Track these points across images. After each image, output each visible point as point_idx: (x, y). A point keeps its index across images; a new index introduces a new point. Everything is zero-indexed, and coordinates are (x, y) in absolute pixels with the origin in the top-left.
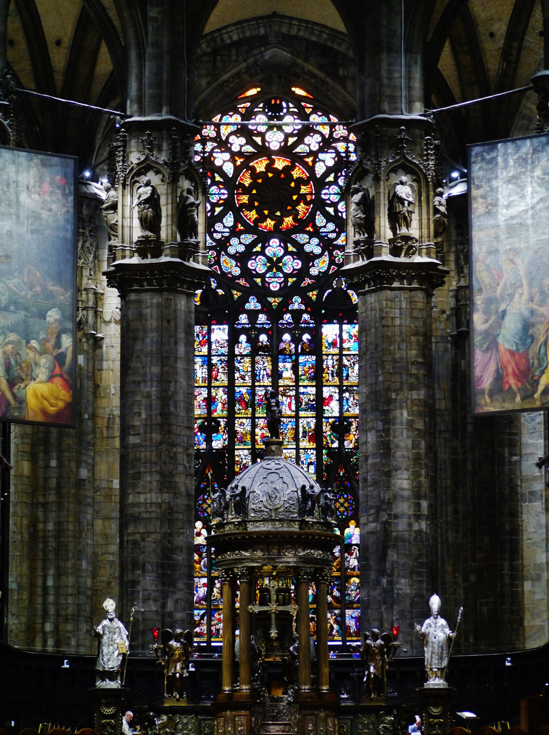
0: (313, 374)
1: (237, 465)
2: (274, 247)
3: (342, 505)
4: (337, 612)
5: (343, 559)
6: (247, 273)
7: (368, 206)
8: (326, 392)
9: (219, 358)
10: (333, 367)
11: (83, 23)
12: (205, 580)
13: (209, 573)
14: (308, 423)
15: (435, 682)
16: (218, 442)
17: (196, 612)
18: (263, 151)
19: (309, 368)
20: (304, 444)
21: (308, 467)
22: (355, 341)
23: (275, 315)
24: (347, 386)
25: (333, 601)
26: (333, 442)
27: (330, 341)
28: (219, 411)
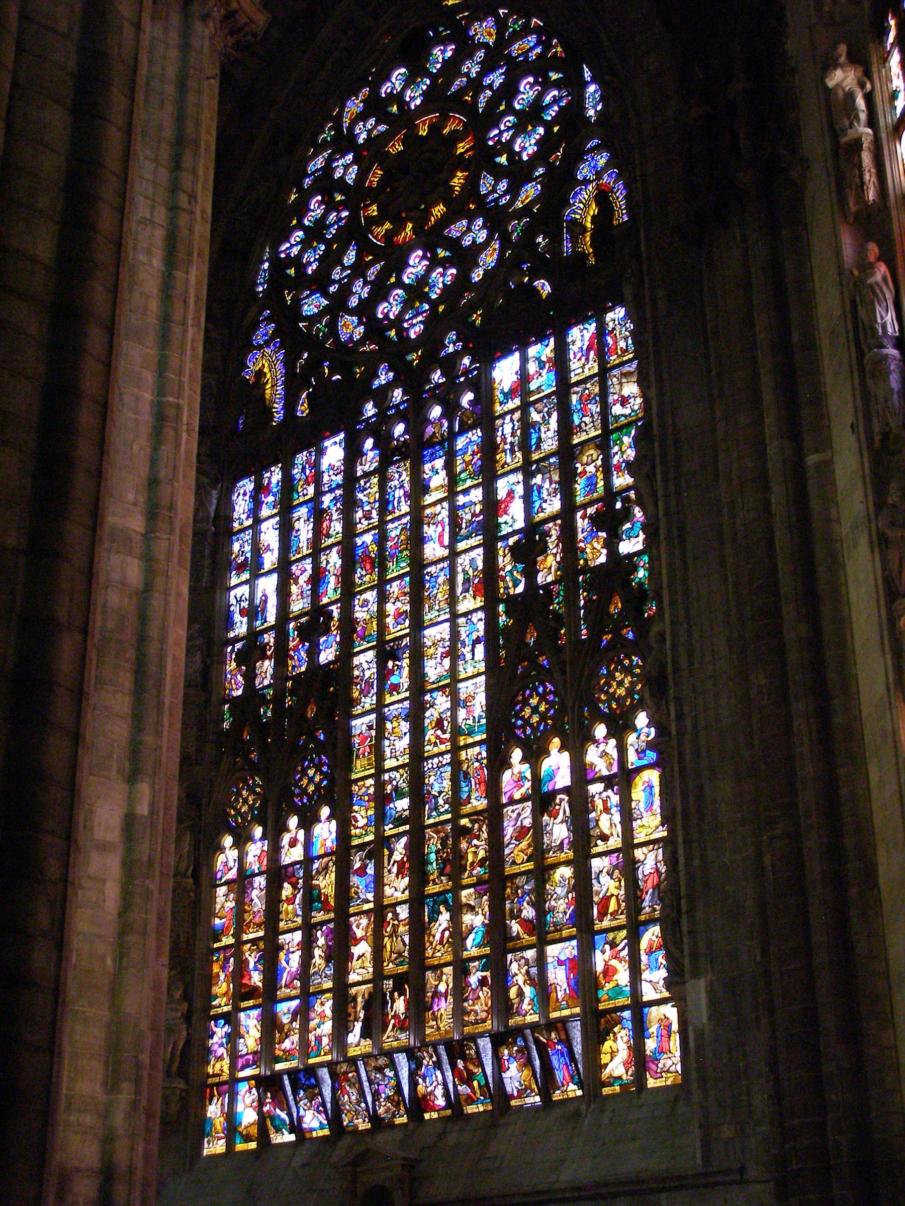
0: (479, 463)
1: (357, 684)
2: (416, 264)
3: (535, 710)
4: (530, 954)
5: (538, 830)
6: (375, 328)
8: (502, 487)
9: (333, 495)
10: (513, 435)
12: (298, 936)
13: (307, 916)
14: (472, 560)
16: (328, 651)
17: (282, 1007)
19: (474, 454)
20: (467, 603)
21: (473, 651)
22: (549, 371)
24: (537, 461)
25: (521, 931)
26: (516, 584)
27: (506, 390)
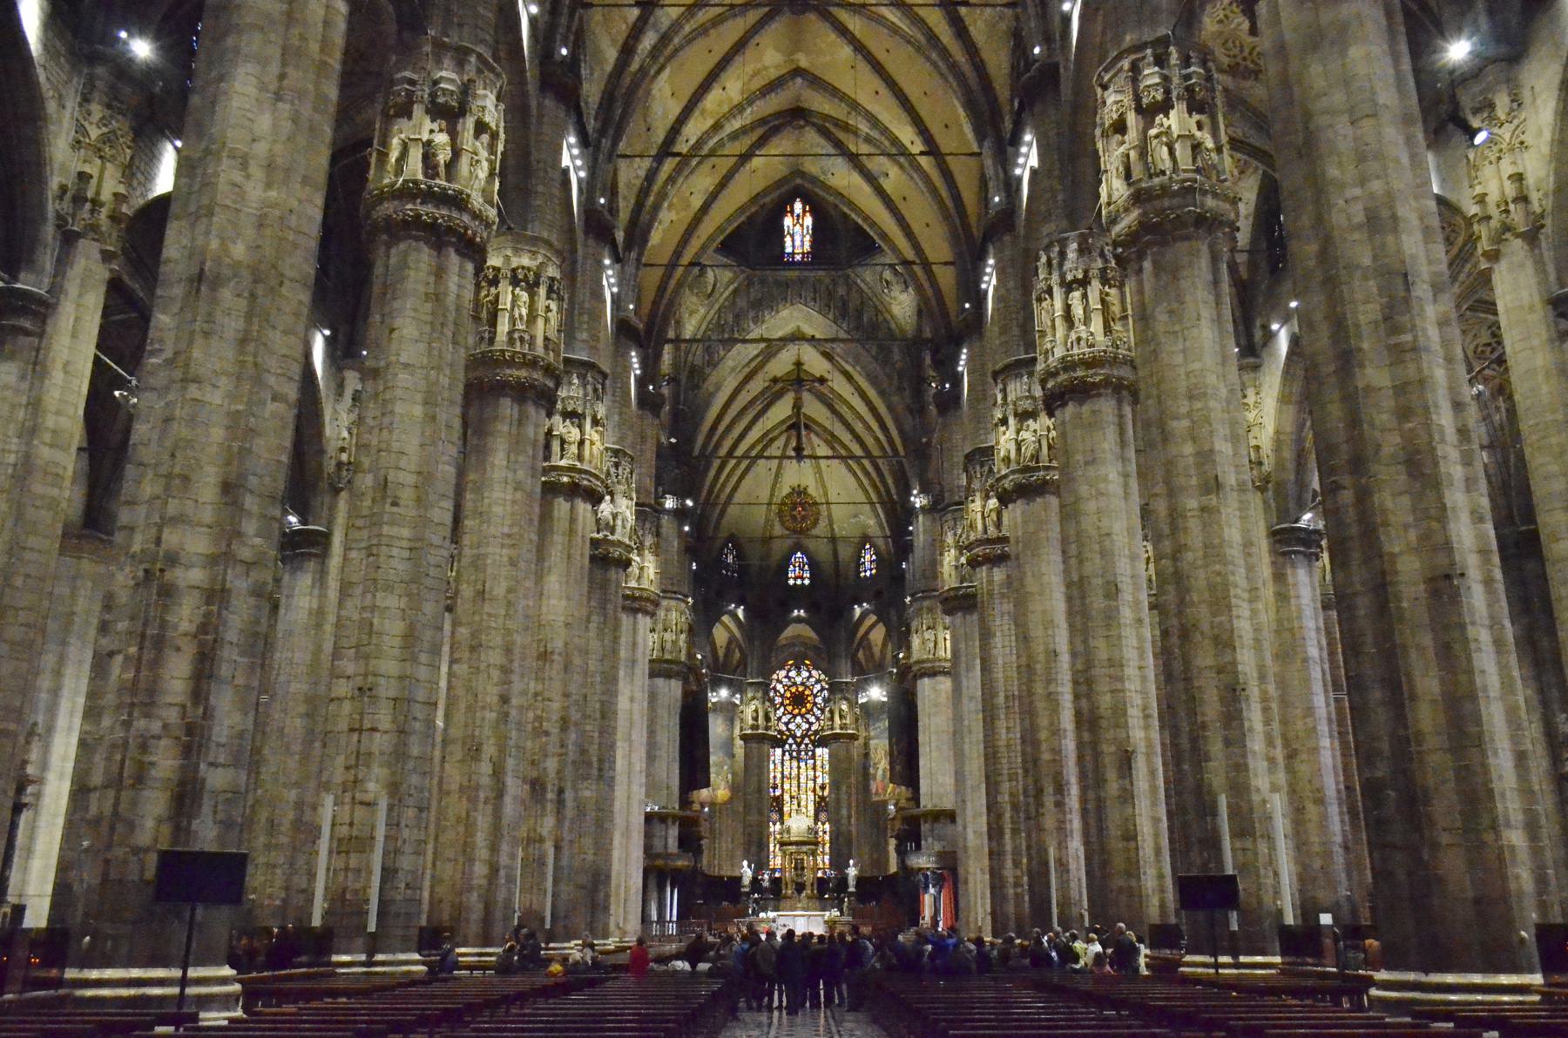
2: (798, 719)
7: (832, 712)
11: (730, 643)
15: (852, 889)
18: (795, 684)
23: (799, 745)
28: (778, 781)
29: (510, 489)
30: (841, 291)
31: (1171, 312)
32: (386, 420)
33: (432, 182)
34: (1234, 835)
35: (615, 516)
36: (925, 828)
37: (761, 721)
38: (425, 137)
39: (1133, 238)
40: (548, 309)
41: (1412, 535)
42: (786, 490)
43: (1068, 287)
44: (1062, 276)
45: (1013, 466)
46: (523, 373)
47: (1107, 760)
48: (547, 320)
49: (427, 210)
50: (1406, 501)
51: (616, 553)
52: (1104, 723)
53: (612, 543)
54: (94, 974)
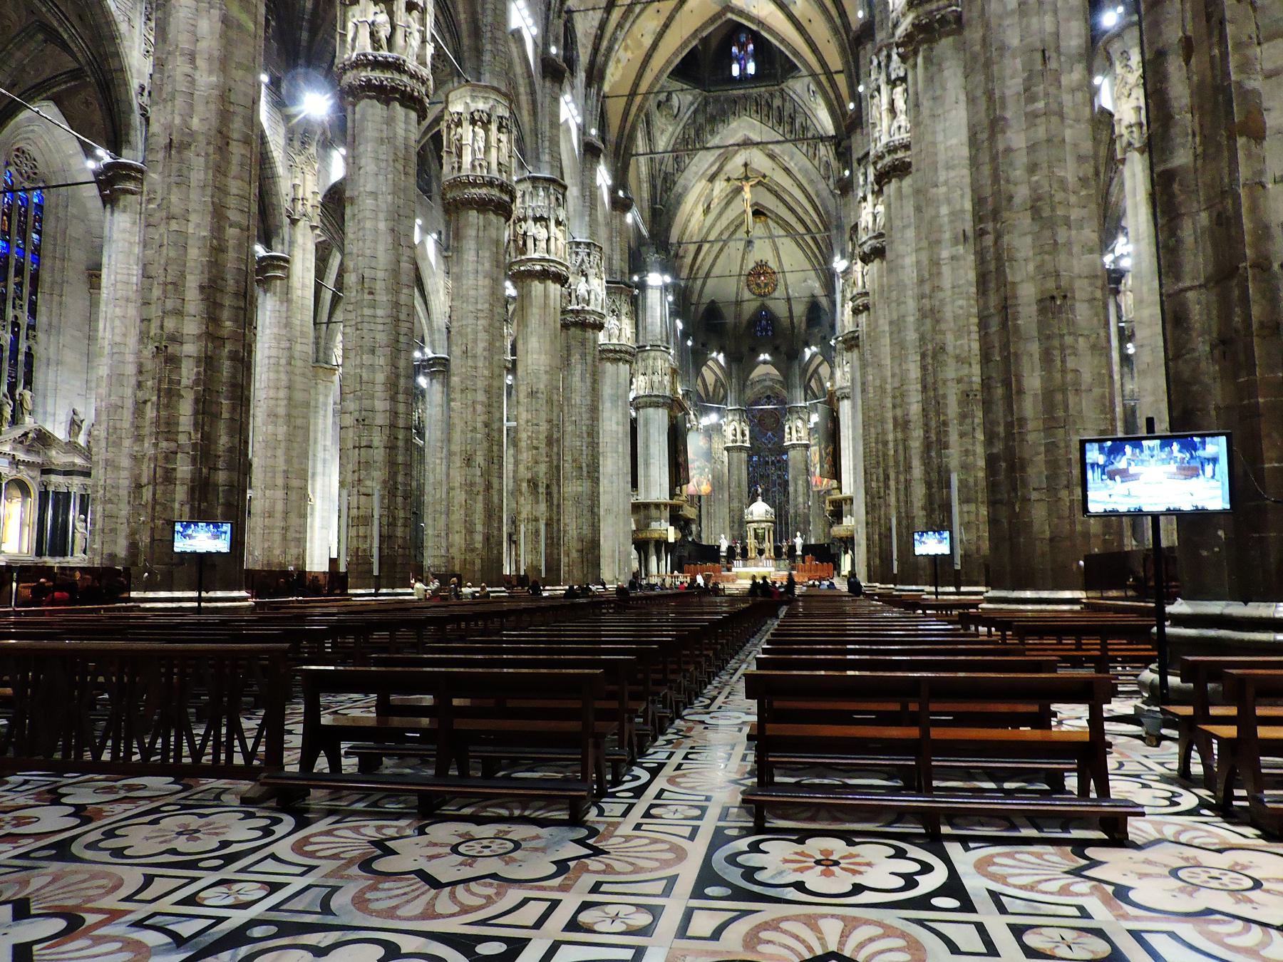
29: (480, 277)
30: (777, 102)
31: (934, 99)
32: (361, 233)
33: (376, 53)
34: (961, 502)
35: (589, 293)
36: (845, 508)
37: (739, 436)
38: (370, 19)
39: (909, 38)
40: (499, 141)
41: (1031, 267)
42: (751, 265)
43: (892, 83)
44: (888, 75)
45: (871, 234)
46: (484, 191)
47: (914, 451)
48: (499, 148)
49: (376, 76)
50: (1028, 240)
51: (591, 319)
52: (912, 425)
53: (588, 312)
54: (151, 595)
